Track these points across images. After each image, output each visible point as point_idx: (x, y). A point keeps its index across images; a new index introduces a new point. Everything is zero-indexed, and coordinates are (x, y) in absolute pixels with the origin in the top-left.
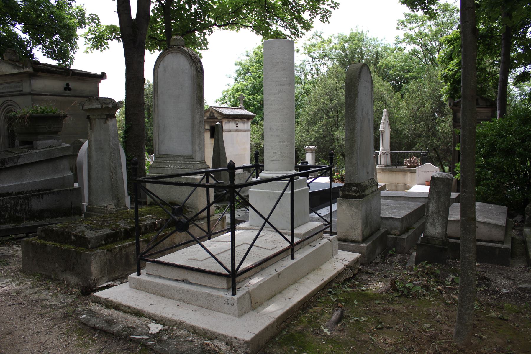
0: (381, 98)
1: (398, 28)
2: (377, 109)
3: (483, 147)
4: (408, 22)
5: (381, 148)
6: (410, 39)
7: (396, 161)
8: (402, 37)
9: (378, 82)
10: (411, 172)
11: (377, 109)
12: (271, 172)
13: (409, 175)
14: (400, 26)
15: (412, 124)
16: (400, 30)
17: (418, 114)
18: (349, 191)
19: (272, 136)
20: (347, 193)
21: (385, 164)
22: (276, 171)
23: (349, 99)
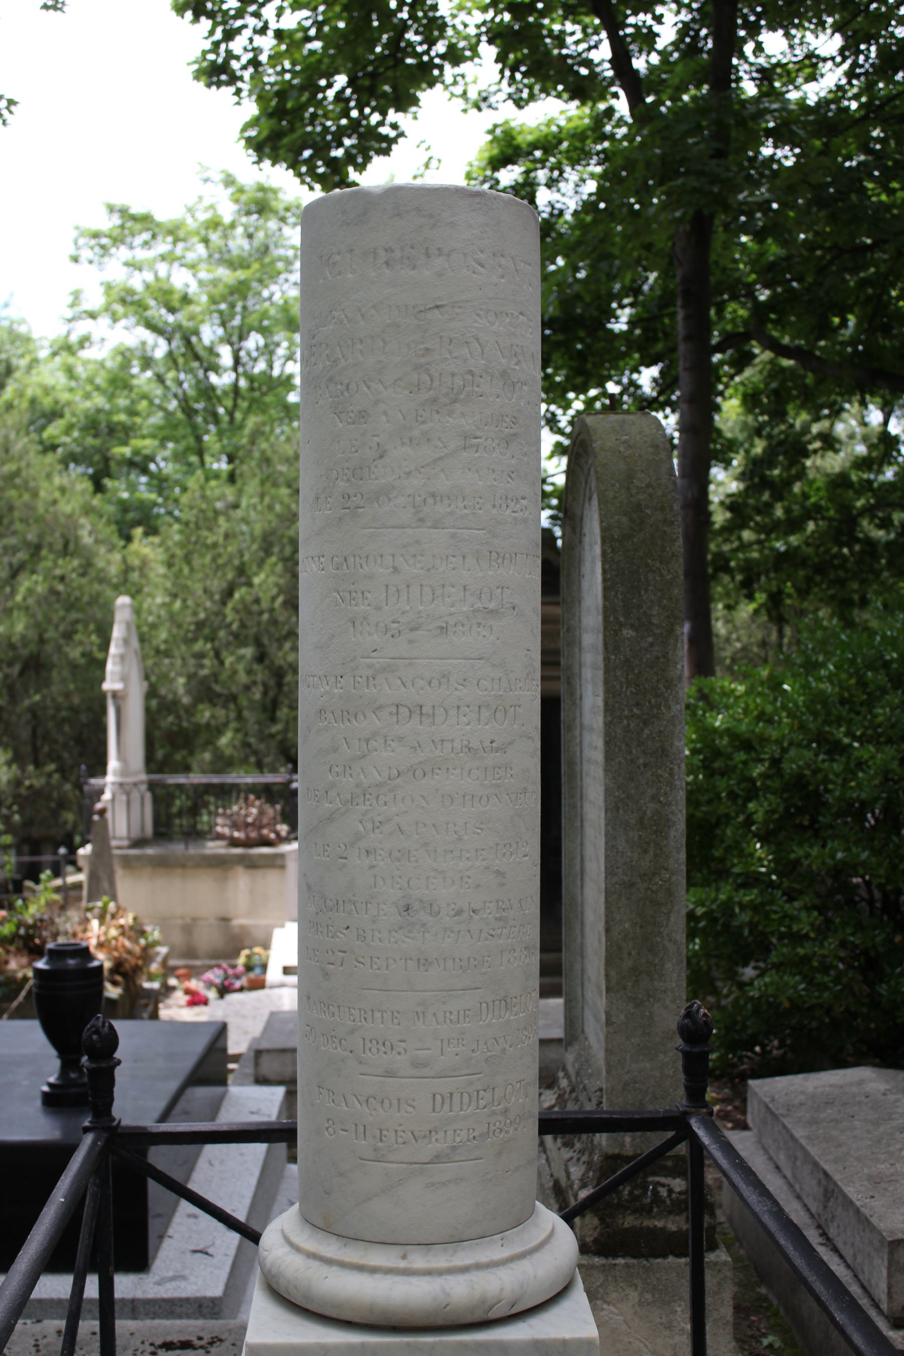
0: (66, 544)
1: (75, 259)
2: (53, 592)
3: (752, 793)
4: (118, 240)
5: (113, 764)
6: (126, 302)
7: (174, 821)
8: (95, 299)
9: (49, 476)
10: (252, 864)
11: (53, 592)
12: (419, 1261)
13: (242, 880)
14: (86, 254)
15: (200, 656)
16: (84, 266)
17: (230, 615)
18: (646, 1211)
19: (424, 962)
20: (629, 1221)
21: (136, 833)
22: (456, 1240)
23: (627, 633)
